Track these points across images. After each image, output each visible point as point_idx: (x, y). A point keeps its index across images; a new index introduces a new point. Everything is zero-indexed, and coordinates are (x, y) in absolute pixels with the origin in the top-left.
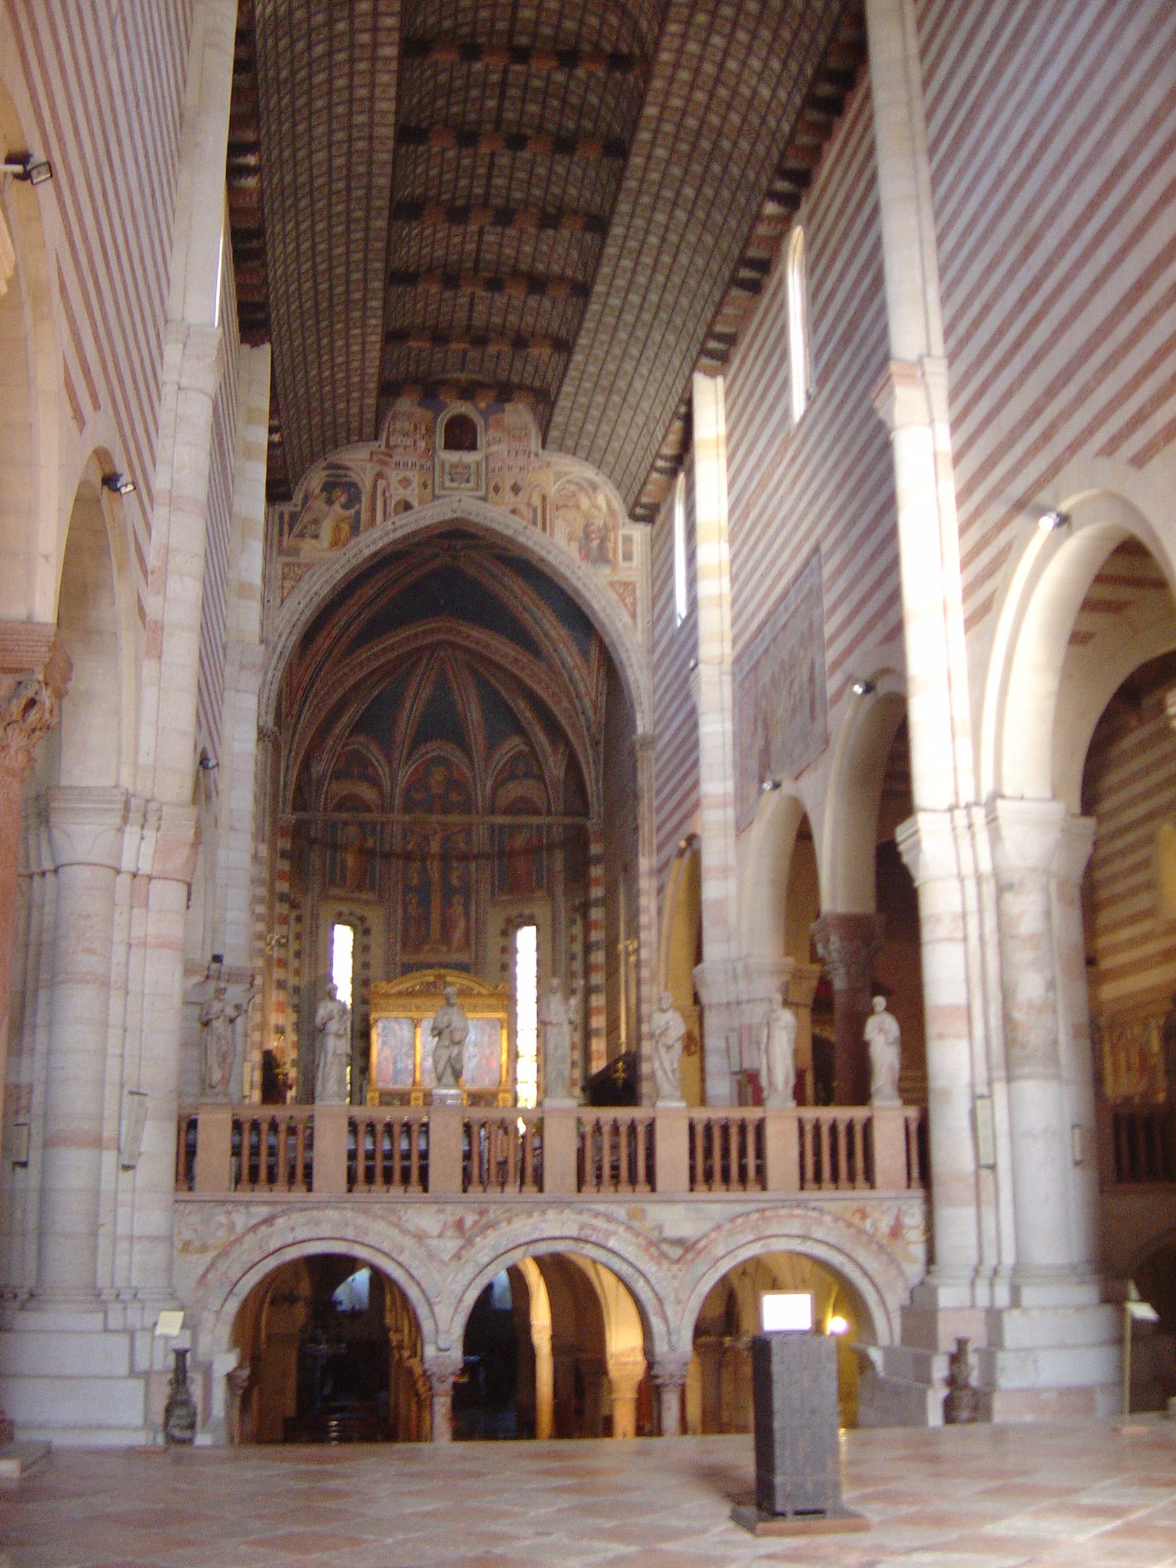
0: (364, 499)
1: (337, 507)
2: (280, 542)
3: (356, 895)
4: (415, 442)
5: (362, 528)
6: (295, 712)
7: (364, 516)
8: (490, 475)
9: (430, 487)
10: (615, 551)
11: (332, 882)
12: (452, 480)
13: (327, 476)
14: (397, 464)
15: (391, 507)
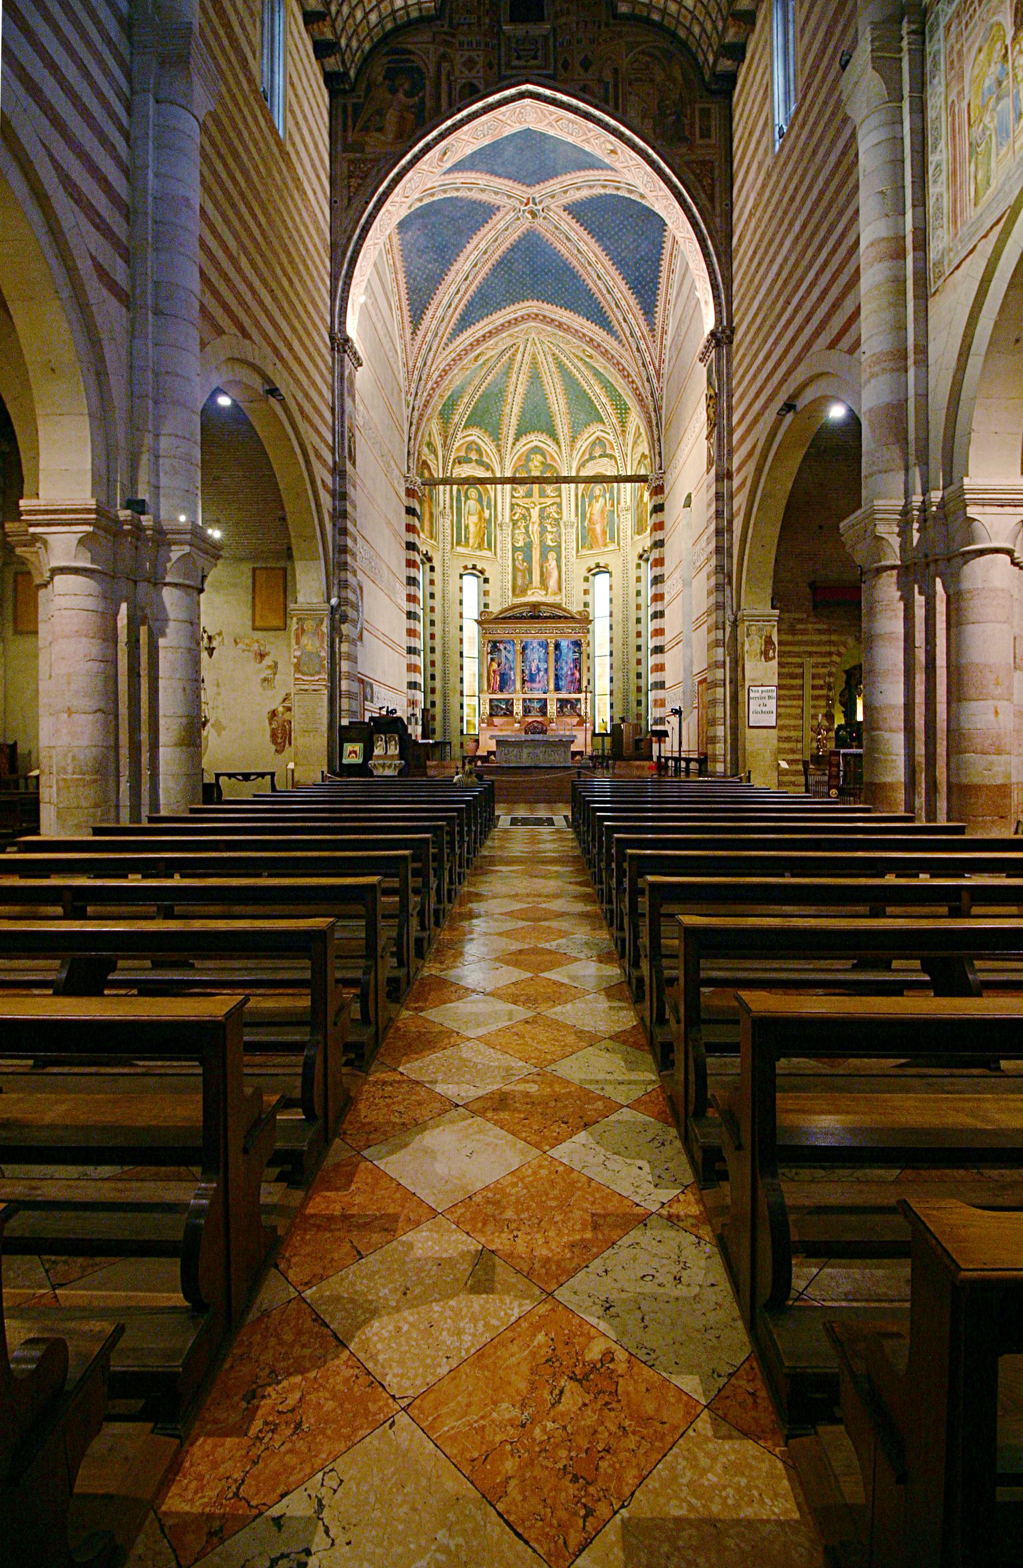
0: (427, 82)
1: (401, 95)
2: (345, 138)
3: (478, 553)
4: (479, 18)
5: (427, 114)
6: (413, 391)
7: (429, 104)
8: (559, 49)
9: (496, 67)
10: (692, 125)
11: (459, 543)
12: (519, 58)
13: (389, 62)
14: (461, 44)
15: (455, 93)
